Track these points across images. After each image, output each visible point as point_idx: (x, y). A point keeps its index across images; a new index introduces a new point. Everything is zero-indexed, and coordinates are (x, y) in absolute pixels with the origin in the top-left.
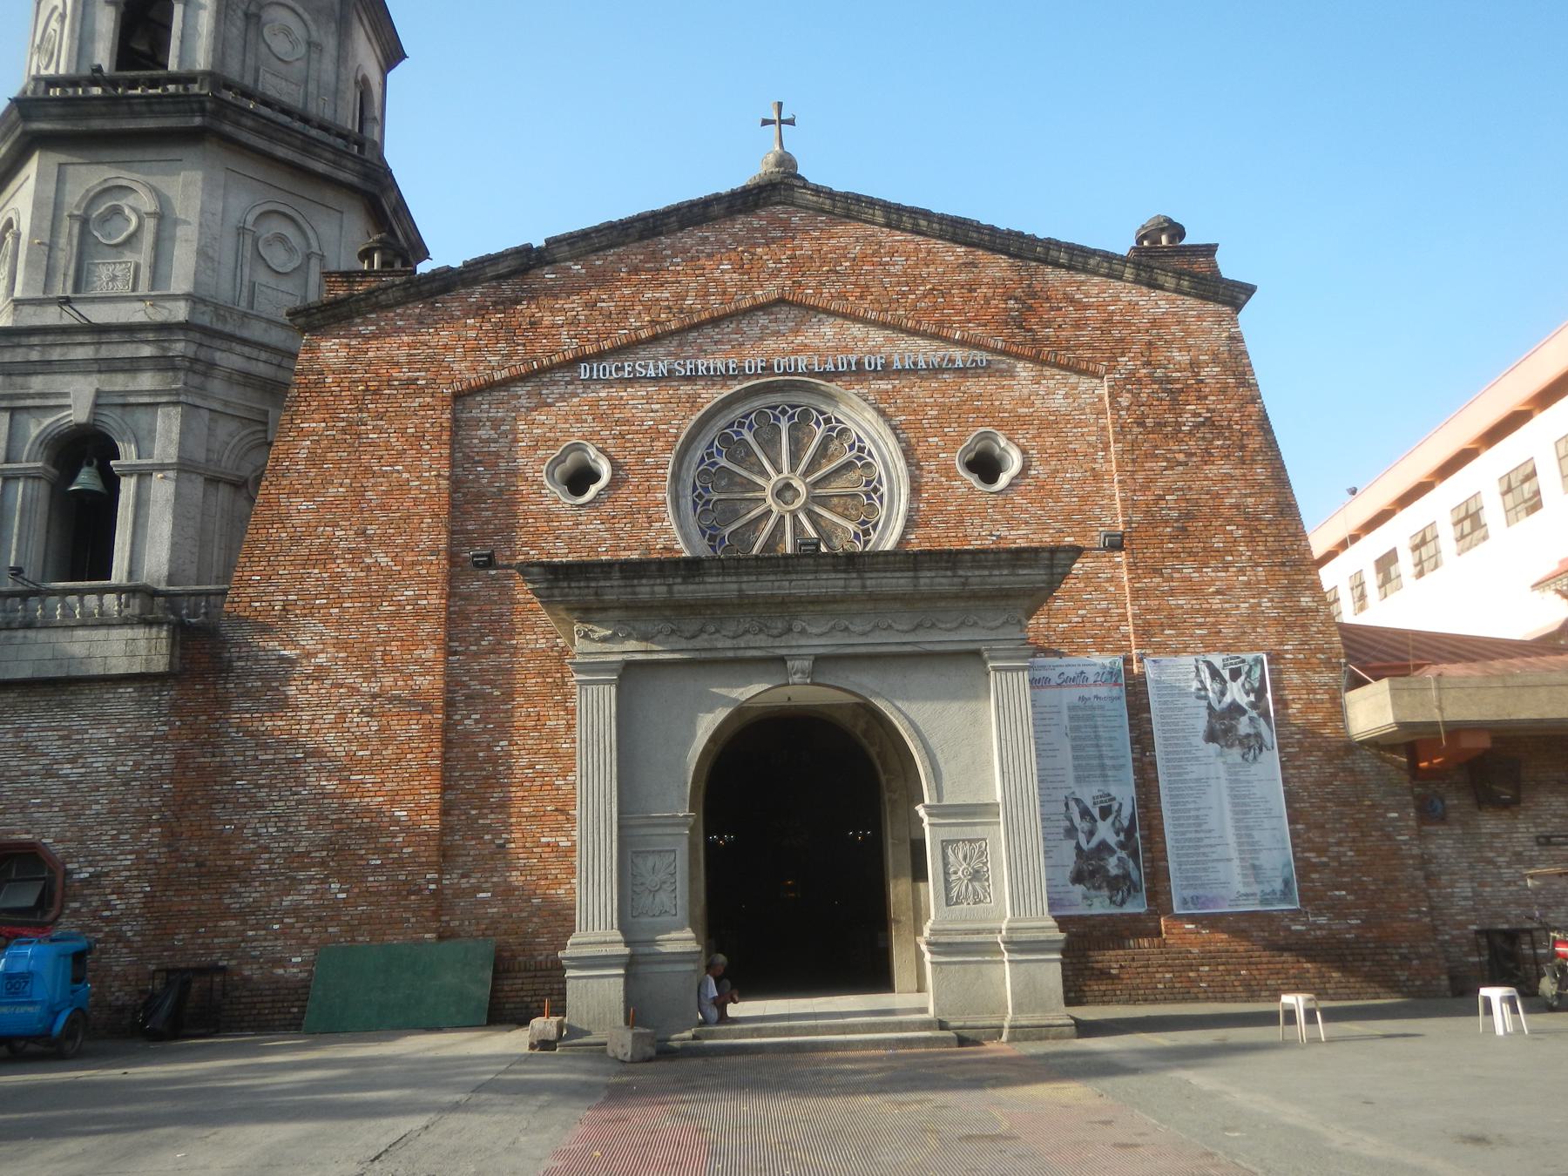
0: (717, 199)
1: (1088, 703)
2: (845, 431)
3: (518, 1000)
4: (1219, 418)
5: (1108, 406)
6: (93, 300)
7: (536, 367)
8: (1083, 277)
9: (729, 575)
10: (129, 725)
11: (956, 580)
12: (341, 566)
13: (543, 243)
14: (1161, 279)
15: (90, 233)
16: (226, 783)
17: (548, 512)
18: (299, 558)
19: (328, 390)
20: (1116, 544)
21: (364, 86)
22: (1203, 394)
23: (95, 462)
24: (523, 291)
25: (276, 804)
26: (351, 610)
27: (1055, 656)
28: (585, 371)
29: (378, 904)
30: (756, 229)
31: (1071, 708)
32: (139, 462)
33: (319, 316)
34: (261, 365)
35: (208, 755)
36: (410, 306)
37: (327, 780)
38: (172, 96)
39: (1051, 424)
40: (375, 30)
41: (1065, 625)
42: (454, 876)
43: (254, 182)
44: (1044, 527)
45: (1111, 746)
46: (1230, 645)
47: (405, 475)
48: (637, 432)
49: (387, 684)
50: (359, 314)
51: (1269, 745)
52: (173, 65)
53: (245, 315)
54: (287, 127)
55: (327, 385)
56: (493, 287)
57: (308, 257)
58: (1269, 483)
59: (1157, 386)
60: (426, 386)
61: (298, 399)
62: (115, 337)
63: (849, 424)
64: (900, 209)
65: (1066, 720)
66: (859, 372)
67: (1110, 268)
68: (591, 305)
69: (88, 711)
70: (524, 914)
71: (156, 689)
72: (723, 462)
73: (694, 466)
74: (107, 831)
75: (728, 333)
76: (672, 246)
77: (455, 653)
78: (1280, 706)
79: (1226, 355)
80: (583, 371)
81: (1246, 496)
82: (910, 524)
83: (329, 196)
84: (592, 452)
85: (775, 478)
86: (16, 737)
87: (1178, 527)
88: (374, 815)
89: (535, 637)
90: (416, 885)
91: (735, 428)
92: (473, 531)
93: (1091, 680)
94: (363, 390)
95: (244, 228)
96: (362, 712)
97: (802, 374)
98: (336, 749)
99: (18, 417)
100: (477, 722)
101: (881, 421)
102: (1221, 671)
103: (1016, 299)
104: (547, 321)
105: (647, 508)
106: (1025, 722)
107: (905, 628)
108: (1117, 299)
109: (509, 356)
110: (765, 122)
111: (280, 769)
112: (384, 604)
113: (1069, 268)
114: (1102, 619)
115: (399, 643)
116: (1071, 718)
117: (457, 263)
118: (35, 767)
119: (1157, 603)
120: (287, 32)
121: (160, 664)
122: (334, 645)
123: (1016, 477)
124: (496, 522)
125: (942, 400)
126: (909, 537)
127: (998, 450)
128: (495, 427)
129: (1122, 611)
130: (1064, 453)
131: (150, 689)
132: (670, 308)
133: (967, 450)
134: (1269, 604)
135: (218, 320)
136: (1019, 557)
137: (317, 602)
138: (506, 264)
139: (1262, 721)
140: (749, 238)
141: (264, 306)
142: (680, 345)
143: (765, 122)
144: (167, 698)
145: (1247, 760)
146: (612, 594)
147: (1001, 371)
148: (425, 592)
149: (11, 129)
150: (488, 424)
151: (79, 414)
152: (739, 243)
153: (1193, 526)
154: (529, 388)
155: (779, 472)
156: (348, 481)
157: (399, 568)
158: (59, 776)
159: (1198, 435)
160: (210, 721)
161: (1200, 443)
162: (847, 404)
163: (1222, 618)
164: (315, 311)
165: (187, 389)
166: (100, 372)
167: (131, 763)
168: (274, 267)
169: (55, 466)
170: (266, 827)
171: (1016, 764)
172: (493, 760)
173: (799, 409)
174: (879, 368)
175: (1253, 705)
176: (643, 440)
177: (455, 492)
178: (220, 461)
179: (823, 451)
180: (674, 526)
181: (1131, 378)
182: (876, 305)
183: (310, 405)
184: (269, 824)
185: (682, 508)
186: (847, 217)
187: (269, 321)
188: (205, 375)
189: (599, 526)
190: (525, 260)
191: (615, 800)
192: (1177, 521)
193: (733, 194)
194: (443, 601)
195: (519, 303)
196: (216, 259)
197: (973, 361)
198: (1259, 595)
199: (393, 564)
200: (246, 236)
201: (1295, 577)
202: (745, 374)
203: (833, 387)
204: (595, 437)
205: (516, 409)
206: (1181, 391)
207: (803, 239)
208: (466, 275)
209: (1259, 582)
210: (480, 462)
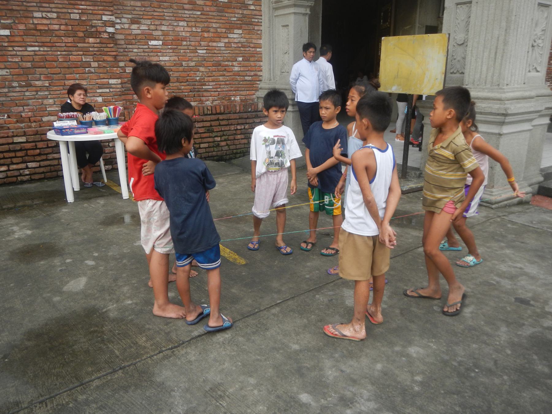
3: (210, 140)
29: (52, 45)
42: (124, 20)
70: (193, 64)
90: (92, 26)
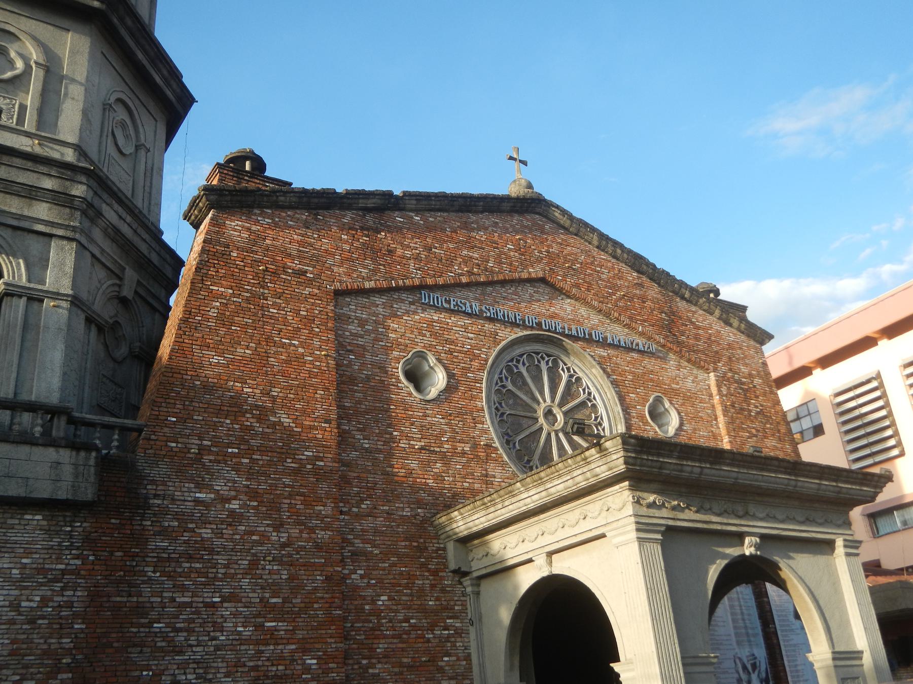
2: (579, 379)
7: (394, 285)
8: (694, 308)
10: (38, 556)
14: (732, 320)
16: (143, 626)
17: (403, 402)
18: (213, 407)
19: (233, 262)
25: (194, 649)
26: (261, 463)
30: (526, 227)
32: (32, 285)
33: (229, 198)
34: (126, 225)
35: (124, 594)
36: (298, 211)
37: (243, 626)
39: (688, 398)
47: (301, 350)
48: (460, 352)
49: (293, 535)
50: (260, 207)
55: (232, 258)
61: (208, 264)
62: (17, 162)
63: (580, 374)
66: (589, 340)
68: (429, 249)
71: (68, 519)
73: (494, 385)
74: (8, 676)
76: (476, 222)
77: (342, 513)
79: (762, 373)
80: (425, 297)
83: (151, 105)
84: (432, 360)
85: (543, 405)
88: (288, 662)
89: (401, 505)
92: (349, 408)
94: (263, 270)
95: (111, 106)
98: (251, 595)
100: (362, 577)
105: (472, 412)
109: (375, 271)
110: (511, 158)
112: (289, 460)
113: (688, 301)
115: (302, 498)
117: (340, 190)
121: (88, 493)
122: (246, 494)
123: (677, 430)
130: (696, 418)
131: (61, 519)
137: (230, 450)
138: (374, 201)
140: (522, 231)
142: (483, 294)
143: (511, 158)
144: (80, 529)
148: (321, 455)
150: (356, 321)
152: (517, 233)
154: (384, 301)
155: (545, 401)
156: (253, 345)
157: (299, 430)
160: (125, 558)
162: (581, 361)
164: (227, 193)
165: (82, 231)
167: (38, 599)
170: (185, 673)
172: (377, 613)
173: (552, 358)
174: (601, 340)
179: (569, 393)
180: (491, 429)
183: (218, 272)
184: (188, 671)
186: (576, 235)
188: (92, 221)
189: (441, 420)
191: (676, 641)
193: (518, 199)
194: (336, 465)
195: (379, 233)
199: (293, 425)
203: (577, 346)
204: (433, 350)
205: (377, 315)
207: (553, 242)
208: (345, 200)
210: (351, 351)
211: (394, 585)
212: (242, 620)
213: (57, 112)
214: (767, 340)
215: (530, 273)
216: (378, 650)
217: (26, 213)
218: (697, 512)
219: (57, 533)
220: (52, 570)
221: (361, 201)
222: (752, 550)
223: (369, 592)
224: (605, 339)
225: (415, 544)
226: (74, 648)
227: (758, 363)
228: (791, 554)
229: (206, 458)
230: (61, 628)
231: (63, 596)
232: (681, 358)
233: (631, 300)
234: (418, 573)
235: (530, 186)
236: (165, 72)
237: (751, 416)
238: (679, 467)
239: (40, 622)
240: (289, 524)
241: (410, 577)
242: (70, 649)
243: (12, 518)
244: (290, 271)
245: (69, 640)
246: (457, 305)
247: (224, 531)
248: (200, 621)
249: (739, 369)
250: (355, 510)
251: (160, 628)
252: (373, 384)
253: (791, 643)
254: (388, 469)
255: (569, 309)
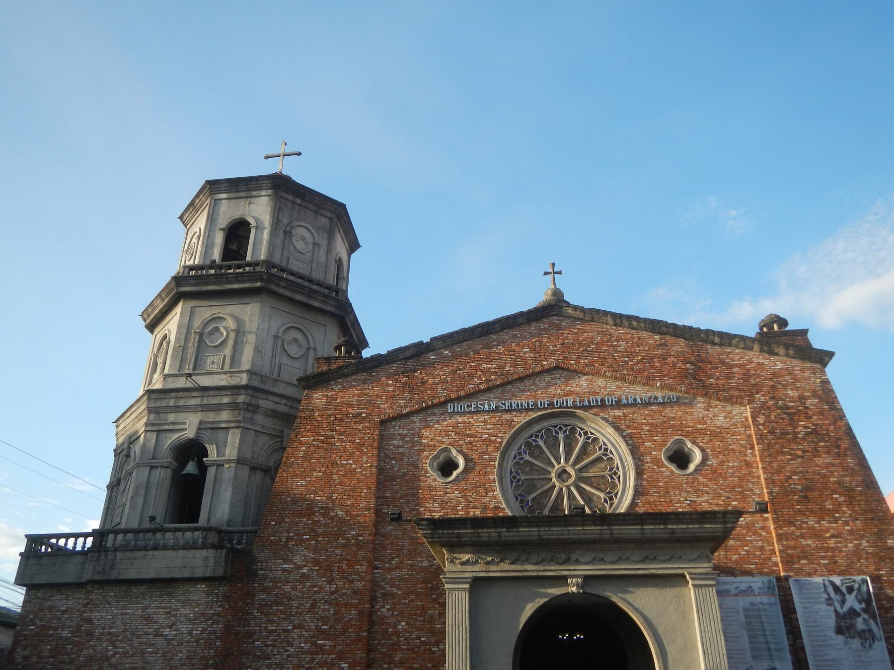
0: (521, 314)
1: (756, 607)
2: (596, 440)
4: (821, 429)
5: (751, 423)
6: (201, 374)
8: (728, 350)
9: (533, 526)
10: (201, 607)
11: (667, 530)
12: (318, 517)
13: (429, 340)
14: (776, 350)
15: (203, 340)
17: (430, 486)
20: (762, 509)
21: (339, 262)
22: (808, 415)
23: (196, 459)
24: (418, 365)
25: (276, 657)
26: (322, 542)
27: (732, 576)
28: (451, 408)
30: (542, 330)
31: (746, 610)
32: (218, 459)
33: (313, 381)
34: (282, 406)
35: (241, 626)
36: (359, 375)
37: (305, 644)
38: (247, 273)
39: (718, 434)
40: (346, 235)
41: (736, 556)
43: (284, 313)
44: (719, 496)
45: (773, 635)
46: (844, 570)
47: (354, 466)
48: (479, 441)
49: (339, 586)
50: (334, 379)
51: (879, 638)
52: (249, 258)
53: (275, 380)
54: (302, 285)
56: (402, 364)
57: (308, 349)
58: (857, 468)
59: (780, 411)
60: (366, 417)
62: (211, 393)
63: (598, 435)
64: (621, 316)
65: (743, 619)
66: (603, 405)
67: (745, 344)
68: (454, 372)
69: (181, 597)
72: (527, 458)
73: (511, 460)
75: (529, 386)
76: (497, 340)
77: (378, 568)
78: (882, 611)
79: (820, 392)
81: (845, 476)
82: (637, 493)
83: (321, 318)
84: (454, 452)
86: (143, 612)
87: (802, 496)
89: (422, 559)
91: (533, 438)
92: (389, 497)
93: (757, 592)
96: (326, 602)
97: (569, 408)
98: (310, 624)
99: (162, 435)
100: (388, 610)
101: (617, 434)
102: (841, 588)
103: (691, 363)
104: (431, 381)
106: (716, 620)
107: (637, 559)
108: (750, 362)
109: (410, 400)
110: (546, 273)
111: (279, 635)
112: (340, 539)
113: (721, 345)
114: (760, 553)
116: (746, 616)
117: (384, 352)
118: (151, 630)
119: (794, 543)
120: (303, 239)
121: (220, 573)
123: (698, 466)
124: (402, 492)
125: (652, 421)
126: (637, 501)
127: (687, 450)
128: (402, 439)
129: (772, 548)
130: (727, 451)
131: (214, 586)
132: (496, 372)
133: (668, 450)
134: (867, 544)
135: (262, 382)
136: (704, 516)
137: (304, 537)
138: (409, 352)
139: (872, 622)
140: (539, 334)
141: (285, 376)
143: (546, 273)
145: (865, 647)
146: (467, 537)
147: (685, 404)
148: (362, 532)
149: (170, 292)
150: (398, 437)
151: (190, 434)
153: (810, 495)
155: (559, 463)
156: (323, 469)
158: (162, 635)
159: (809, 440)
161: (811, 444)
162: (597, 424)
163: (837, 553)
166: (202, 411)
167: (200, 629)
168: (290, 354)
169: (176, 461)
171: (713, 648)
172: (397, 633)
173: (569, 427)
174: (614, 403)
175: (865, 611)
176: (482, 446)
177: (380, 475)
178: (258, 458)
179: (584, 451)
181: (763, 406)
182: (611, 369)
183: (306, 428)
185: (504, 483)
186: (593, 321)
187: (287, 383)
189: (458, 495)
190: (420, 349)
191: (468, 663)
192: (801, 492)
193: (530, 312)
194: (372, 538)
196: (263, 352)
197: (669, 398)
198: (862, 537)
200: (279, 340)
201: (882, 527)
202: (538, 408)
205: (413, 429)
206: (795, 414)
207: (568, 334)
208: (389, 358)
209: (859, 530)
210: (393, 458)
211: (411, 615)
212: (303, 639)
213: (242, 353)
214: (827, 359)
215: (543, 366)
216: (396, 659)
217: (217, 419)
218: (513, 563)
219: (211, 594)
220: (207, 614)
221: (400, 355)
222: (574, 589)
223: (393, 620)
224: (619, 402)
225: (430, 585)
226: (216, 655)
227: (815, 382)
228: (630, 589)
229: (290, 544)
230: (210, 645)
231: (212, 627)
232: (710, 398)
233: (650, 361)
234: (430, 606)
235: (557, 294)
236: (321, 298)
237: (797, 437)
238: (476, 535)
239: (201, 641)
240: (337, 579)
241: (423, 608)
242: (214, 656)
243: (192, 587)
244: (351, 416)
245: (213, 651)
246: (477, 407)
247: (298, 587)
248: (280, 640)
249: (786, 395)
250: (387, 565)
251: (259, 644)
252: (407, 478)
253: (825, 658)
254: (413, 535)
255: (585, 384)
